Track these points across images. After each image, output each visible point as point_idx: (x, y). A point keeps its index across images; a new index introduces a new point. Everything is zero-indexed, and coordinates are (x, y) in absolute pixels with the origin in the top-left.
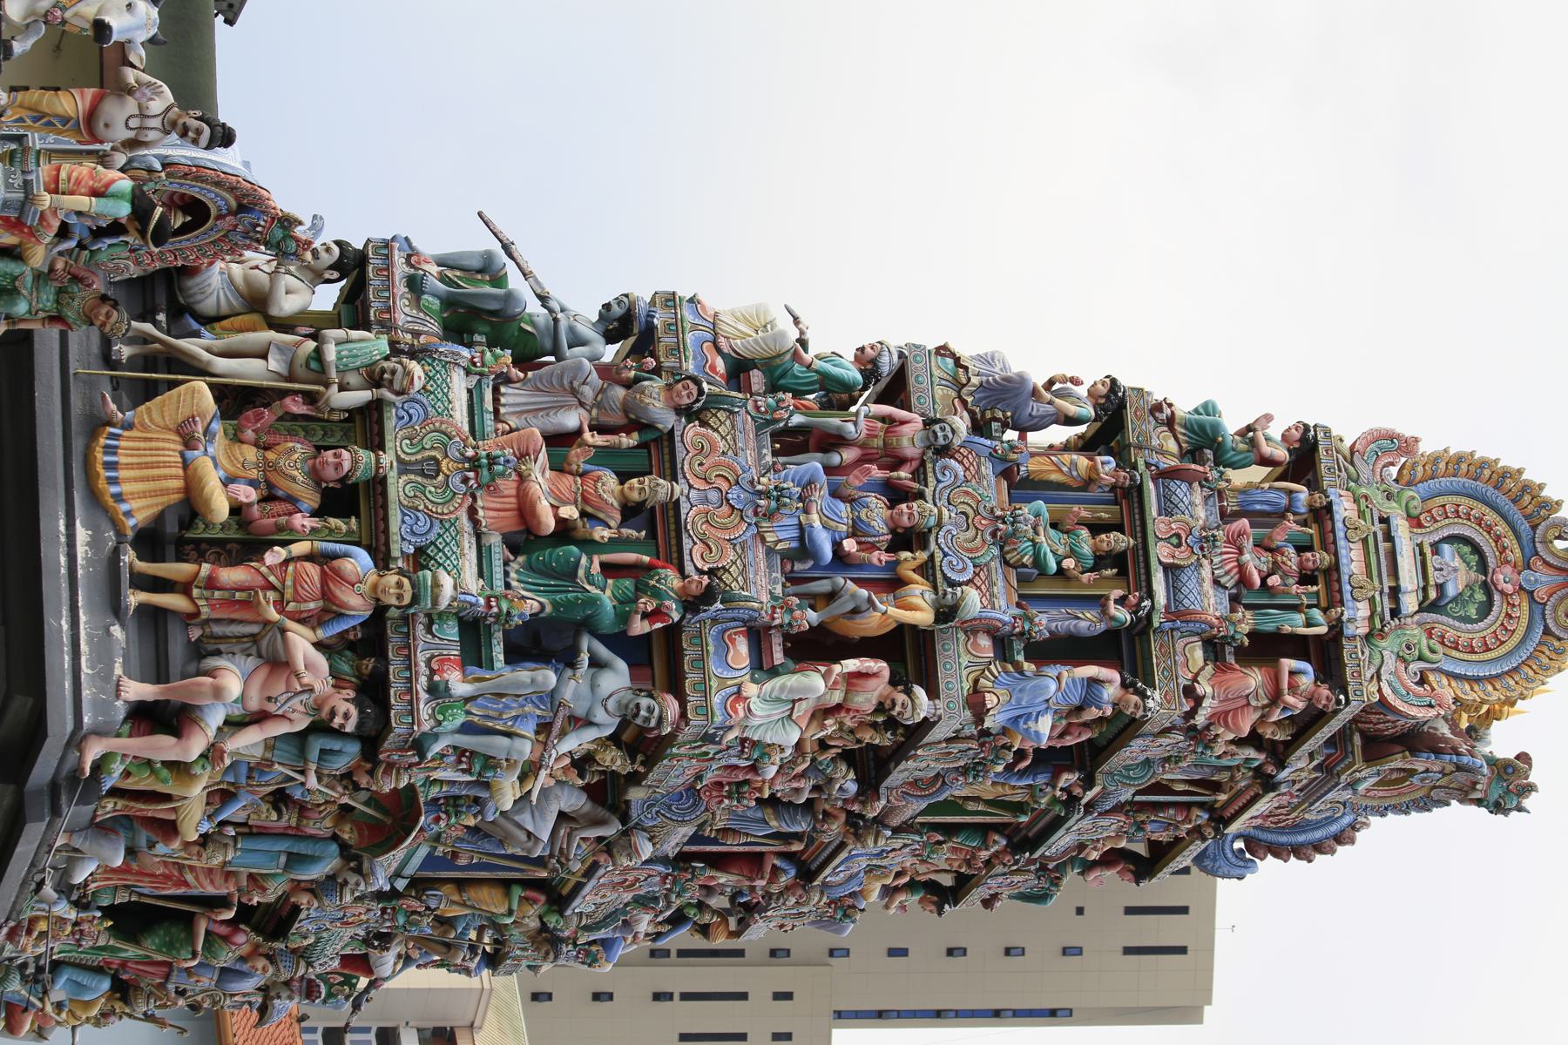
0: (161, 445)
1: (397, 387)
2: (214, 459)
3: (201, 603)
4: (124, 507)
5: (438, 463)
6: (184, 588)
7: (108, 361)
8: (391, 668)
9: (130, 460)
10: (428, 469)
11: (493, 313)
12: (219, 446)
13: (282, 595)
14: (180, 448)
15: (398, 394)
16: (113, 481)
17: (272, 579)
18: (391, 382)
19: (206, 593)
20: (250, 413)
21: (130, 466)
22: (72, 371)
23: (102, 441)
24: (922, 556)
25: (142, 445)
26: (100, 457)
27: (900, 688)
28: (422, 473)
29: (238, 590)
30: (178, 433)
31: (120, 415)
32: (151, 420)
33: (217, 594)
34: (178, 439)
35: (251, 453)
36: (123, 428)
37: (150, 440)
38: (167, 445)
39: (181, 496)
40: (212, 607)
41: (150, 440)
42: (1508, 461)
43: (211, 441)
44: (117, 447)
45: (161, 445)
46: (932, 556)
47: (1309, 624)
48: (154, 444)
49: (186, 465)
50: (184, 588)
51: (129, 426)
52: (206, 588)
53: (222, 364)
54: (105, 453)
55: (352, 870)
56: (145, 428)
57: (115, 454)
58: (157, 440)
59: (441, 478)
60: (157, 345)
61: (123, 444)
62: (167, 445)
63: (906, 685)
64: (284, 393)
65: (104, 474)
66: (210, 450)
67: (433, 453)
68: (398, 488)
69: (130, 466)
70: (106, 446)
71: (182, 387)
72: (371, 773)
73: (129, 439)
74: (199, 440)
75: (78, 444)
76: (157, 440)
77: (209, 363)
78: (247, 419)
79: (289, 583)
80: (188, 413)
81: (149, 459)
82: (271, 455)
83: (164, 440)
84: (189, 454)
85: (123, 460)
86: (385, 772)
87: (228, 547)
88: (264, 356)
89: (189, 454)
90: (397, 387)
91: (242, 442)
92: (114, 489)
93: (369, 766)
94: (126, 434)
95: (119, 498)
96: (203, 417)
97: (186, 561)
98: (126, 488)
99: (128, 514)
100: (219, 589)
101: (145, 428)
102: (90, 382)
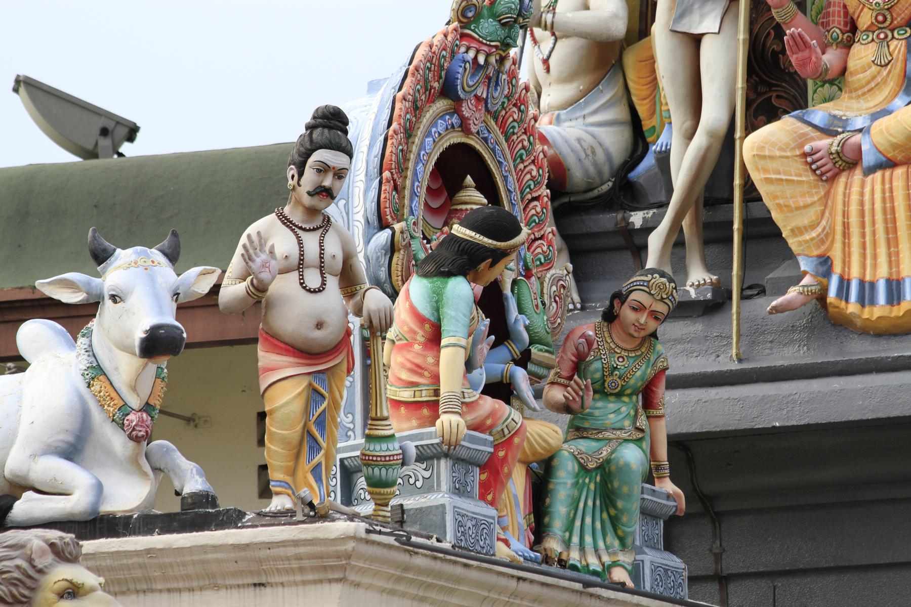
0: (854, 208)
2: (875, 117)
9: (883, 259)
12: (852, 109)
14: (858, 175)
20: (793, 59)
22: (735, 366)
23: (852, 307)
25: (855, 240)
26: (880, 309)
30: (832, 179)
31: (807, 280)
32: (813, 226)
34: (842, 180)
35: (863, 54)
36: (828, 274)
37: (846, 226)
38: (855, 198)
41: (846, 226)
43: (845, 122)
44: (862, 283)
45: (854, 208)
48: (854, 220)
49: (888, 164)
51: (825, 264)
53: (713, 112)
54: (873, 302)
56: (827, 237)
57: (873, 285)
58: (845, 214)
61: (855, 273)
62: (855, 198)
66: (859, 123)
70: (861, 301)
71: (755, 177)
73: (846, 263)
74: (843, 144)
75: (861, 349)
76: (845, 214)
77: (711, 134)
78: (804, 62)
81: (880, 226)
82: (865, 20)
83: (846, 204)
84: (868, 158)
85: (883, 271)
88: (696, 40)
89: (868, 158)
91: (844, 71)
94: (838, 268)
96: (803, 139)
101: (827, 237)
102: (753, 334)
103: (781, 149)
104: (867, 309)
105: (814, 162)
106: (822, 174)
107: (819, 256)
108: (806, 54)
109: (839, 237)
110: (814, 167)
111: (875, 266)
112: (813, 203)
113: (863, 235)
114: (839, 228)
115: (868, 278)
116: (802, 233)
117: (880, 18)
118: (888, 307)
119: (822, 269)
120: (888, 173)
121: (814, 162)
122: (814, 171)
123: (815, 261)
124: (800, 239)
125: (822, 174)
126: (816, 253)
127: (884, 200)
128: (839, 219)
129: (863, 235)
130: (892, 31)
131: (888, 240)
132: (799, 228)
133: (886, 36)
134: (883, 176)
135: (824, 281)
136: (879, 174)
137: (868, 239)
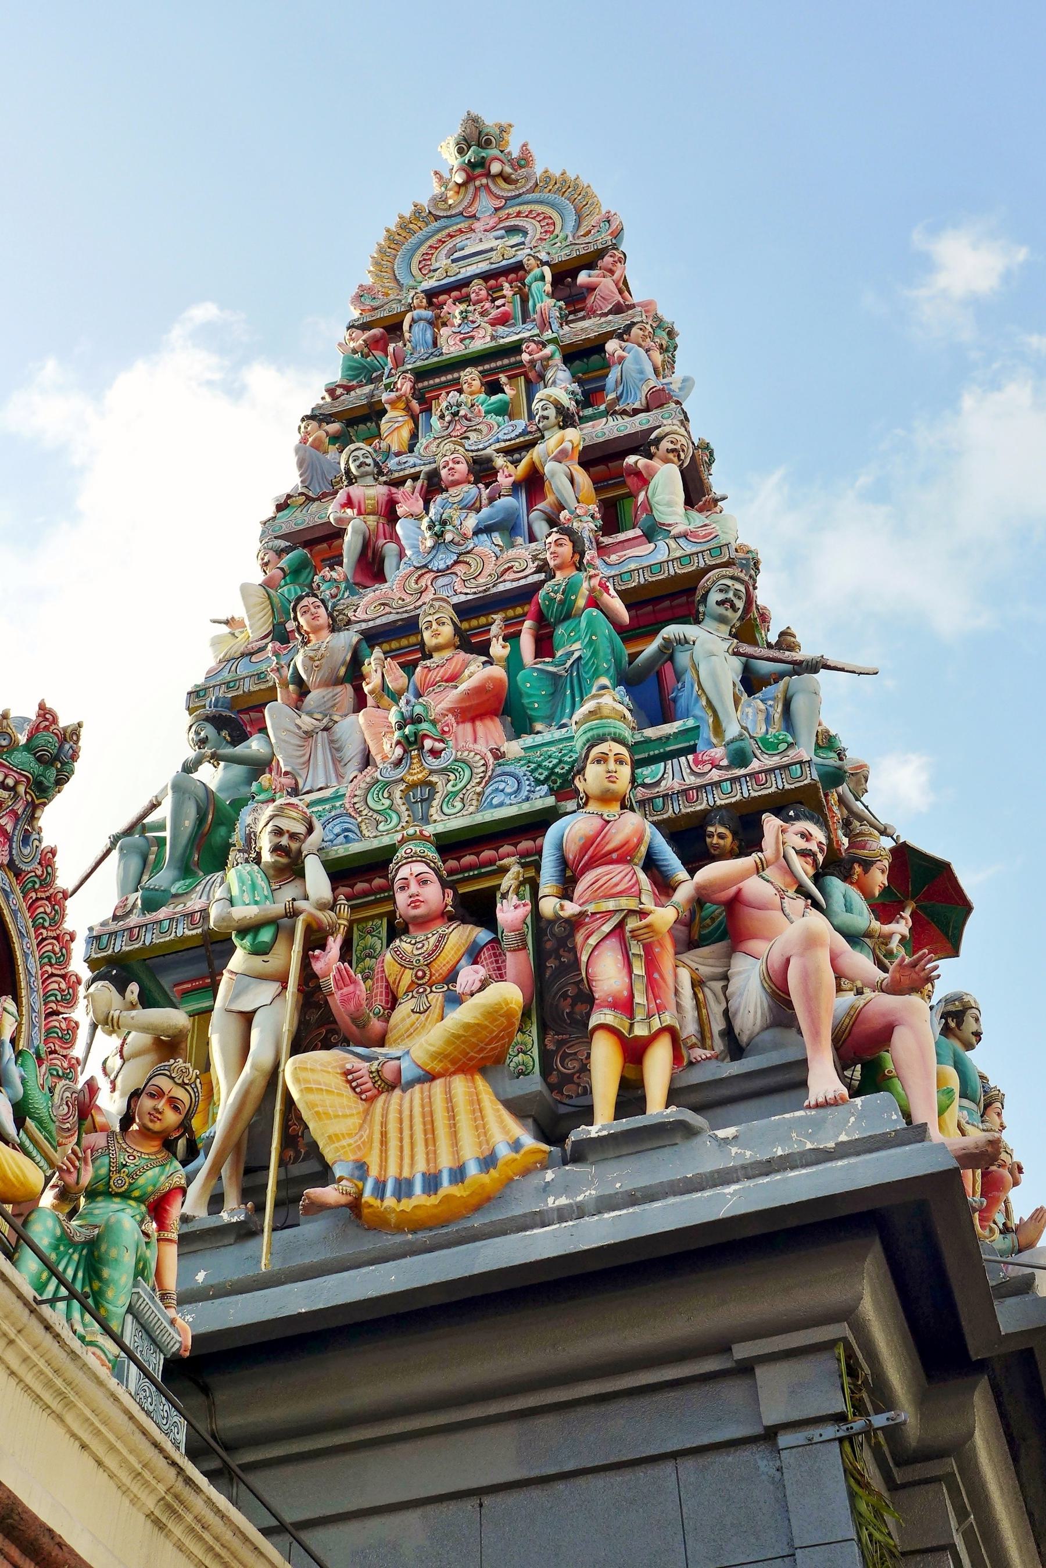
1: (301, 829)
3: (656, 1025)
4: (503, 1152)
5: (412, 786)
6: (634, 1052)
7: (246, 1232)
8: (719, 802)
10: (421, 794)
11: (201, 819)
13: (631, 912)
14: (397, 1092)
15: (310, 830)
16: (458, 1174)
17: (607, 928)
18: (293, 836)
19: (640, 1014)
21: (432, 1155)
24: (500, 461)
27: (653, 449)
28: (427, 801)
29: (630, 971)
30: (371, 1100)
33: (639, 999)
36: (363, 1178)
37: (384, 1135)
39: (478, 1078)
40: (660, 1009)
41: (384, 1135)
42: (381, 237)
46: (498, 451)
47: (543, 278)
50: (634, 1052)
51: (361, 1168)
52: (631, 1016)
54: (410, 1195)
55: (959, 1025)
58: (384, 1124)
59: (434, 778)
60: (225, 1171)
61: (392, 1171)
63: (650, 444)
64: (308, 975)
65: (446, 1188)
67: (398, 794)
68: (450, 818)
69: (432, 1155)
71: (295, 1095)
72: (867, 865)
76: (384, 1124)
79: (611, 905)
80: (340, 1080)
81: (418, 1128)
85: (421, 1166)
86: (864, 848)
87: (551, 1047)
90: (301, 829)
92: (472, 1169)
93: (858, 869)
94: (374, 1171)
95: (488, 1162)
97: (585, 1068)
98: (470, 1153)
99: (516, 1146)
100: (632, 996)
103: (322, 1065)
104: (404, 1201)
105: (354, 1080)
106: (361, 1093)
107: (356, 1161)
108: (351, 988)
109: (377, 1144)
110: (354, 1084)
111: (412, 1165)
112: (352, 1115)
113: (401, 1140)
114: (377, 1136)
115: (406, 1174)
116: (339, 1140)
117: (420, 974)
118: (425, 1196)
119: (357, 1173)
120: (426, 1085)
121: (354, 1080)
122: (354, 1089)
123: (351, 1165)
124: (336, 1145)
125: (361, 1093)
126: (352, 1158)
127: (423, 1106)
128: (377, 1128)
129: (401, 1140)
130: (431, 987)
131: (426, 1141)
132: (336, 1135)
133: (425, 990)
134: (422, 1089)
135: (360, 1184)
136: (417, 1087)
137: (406, 1140)
